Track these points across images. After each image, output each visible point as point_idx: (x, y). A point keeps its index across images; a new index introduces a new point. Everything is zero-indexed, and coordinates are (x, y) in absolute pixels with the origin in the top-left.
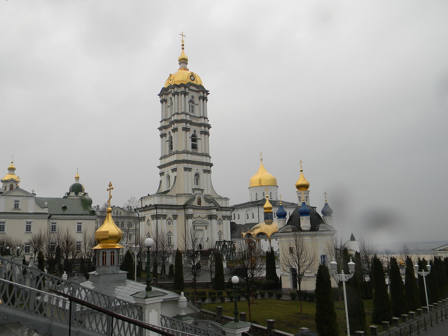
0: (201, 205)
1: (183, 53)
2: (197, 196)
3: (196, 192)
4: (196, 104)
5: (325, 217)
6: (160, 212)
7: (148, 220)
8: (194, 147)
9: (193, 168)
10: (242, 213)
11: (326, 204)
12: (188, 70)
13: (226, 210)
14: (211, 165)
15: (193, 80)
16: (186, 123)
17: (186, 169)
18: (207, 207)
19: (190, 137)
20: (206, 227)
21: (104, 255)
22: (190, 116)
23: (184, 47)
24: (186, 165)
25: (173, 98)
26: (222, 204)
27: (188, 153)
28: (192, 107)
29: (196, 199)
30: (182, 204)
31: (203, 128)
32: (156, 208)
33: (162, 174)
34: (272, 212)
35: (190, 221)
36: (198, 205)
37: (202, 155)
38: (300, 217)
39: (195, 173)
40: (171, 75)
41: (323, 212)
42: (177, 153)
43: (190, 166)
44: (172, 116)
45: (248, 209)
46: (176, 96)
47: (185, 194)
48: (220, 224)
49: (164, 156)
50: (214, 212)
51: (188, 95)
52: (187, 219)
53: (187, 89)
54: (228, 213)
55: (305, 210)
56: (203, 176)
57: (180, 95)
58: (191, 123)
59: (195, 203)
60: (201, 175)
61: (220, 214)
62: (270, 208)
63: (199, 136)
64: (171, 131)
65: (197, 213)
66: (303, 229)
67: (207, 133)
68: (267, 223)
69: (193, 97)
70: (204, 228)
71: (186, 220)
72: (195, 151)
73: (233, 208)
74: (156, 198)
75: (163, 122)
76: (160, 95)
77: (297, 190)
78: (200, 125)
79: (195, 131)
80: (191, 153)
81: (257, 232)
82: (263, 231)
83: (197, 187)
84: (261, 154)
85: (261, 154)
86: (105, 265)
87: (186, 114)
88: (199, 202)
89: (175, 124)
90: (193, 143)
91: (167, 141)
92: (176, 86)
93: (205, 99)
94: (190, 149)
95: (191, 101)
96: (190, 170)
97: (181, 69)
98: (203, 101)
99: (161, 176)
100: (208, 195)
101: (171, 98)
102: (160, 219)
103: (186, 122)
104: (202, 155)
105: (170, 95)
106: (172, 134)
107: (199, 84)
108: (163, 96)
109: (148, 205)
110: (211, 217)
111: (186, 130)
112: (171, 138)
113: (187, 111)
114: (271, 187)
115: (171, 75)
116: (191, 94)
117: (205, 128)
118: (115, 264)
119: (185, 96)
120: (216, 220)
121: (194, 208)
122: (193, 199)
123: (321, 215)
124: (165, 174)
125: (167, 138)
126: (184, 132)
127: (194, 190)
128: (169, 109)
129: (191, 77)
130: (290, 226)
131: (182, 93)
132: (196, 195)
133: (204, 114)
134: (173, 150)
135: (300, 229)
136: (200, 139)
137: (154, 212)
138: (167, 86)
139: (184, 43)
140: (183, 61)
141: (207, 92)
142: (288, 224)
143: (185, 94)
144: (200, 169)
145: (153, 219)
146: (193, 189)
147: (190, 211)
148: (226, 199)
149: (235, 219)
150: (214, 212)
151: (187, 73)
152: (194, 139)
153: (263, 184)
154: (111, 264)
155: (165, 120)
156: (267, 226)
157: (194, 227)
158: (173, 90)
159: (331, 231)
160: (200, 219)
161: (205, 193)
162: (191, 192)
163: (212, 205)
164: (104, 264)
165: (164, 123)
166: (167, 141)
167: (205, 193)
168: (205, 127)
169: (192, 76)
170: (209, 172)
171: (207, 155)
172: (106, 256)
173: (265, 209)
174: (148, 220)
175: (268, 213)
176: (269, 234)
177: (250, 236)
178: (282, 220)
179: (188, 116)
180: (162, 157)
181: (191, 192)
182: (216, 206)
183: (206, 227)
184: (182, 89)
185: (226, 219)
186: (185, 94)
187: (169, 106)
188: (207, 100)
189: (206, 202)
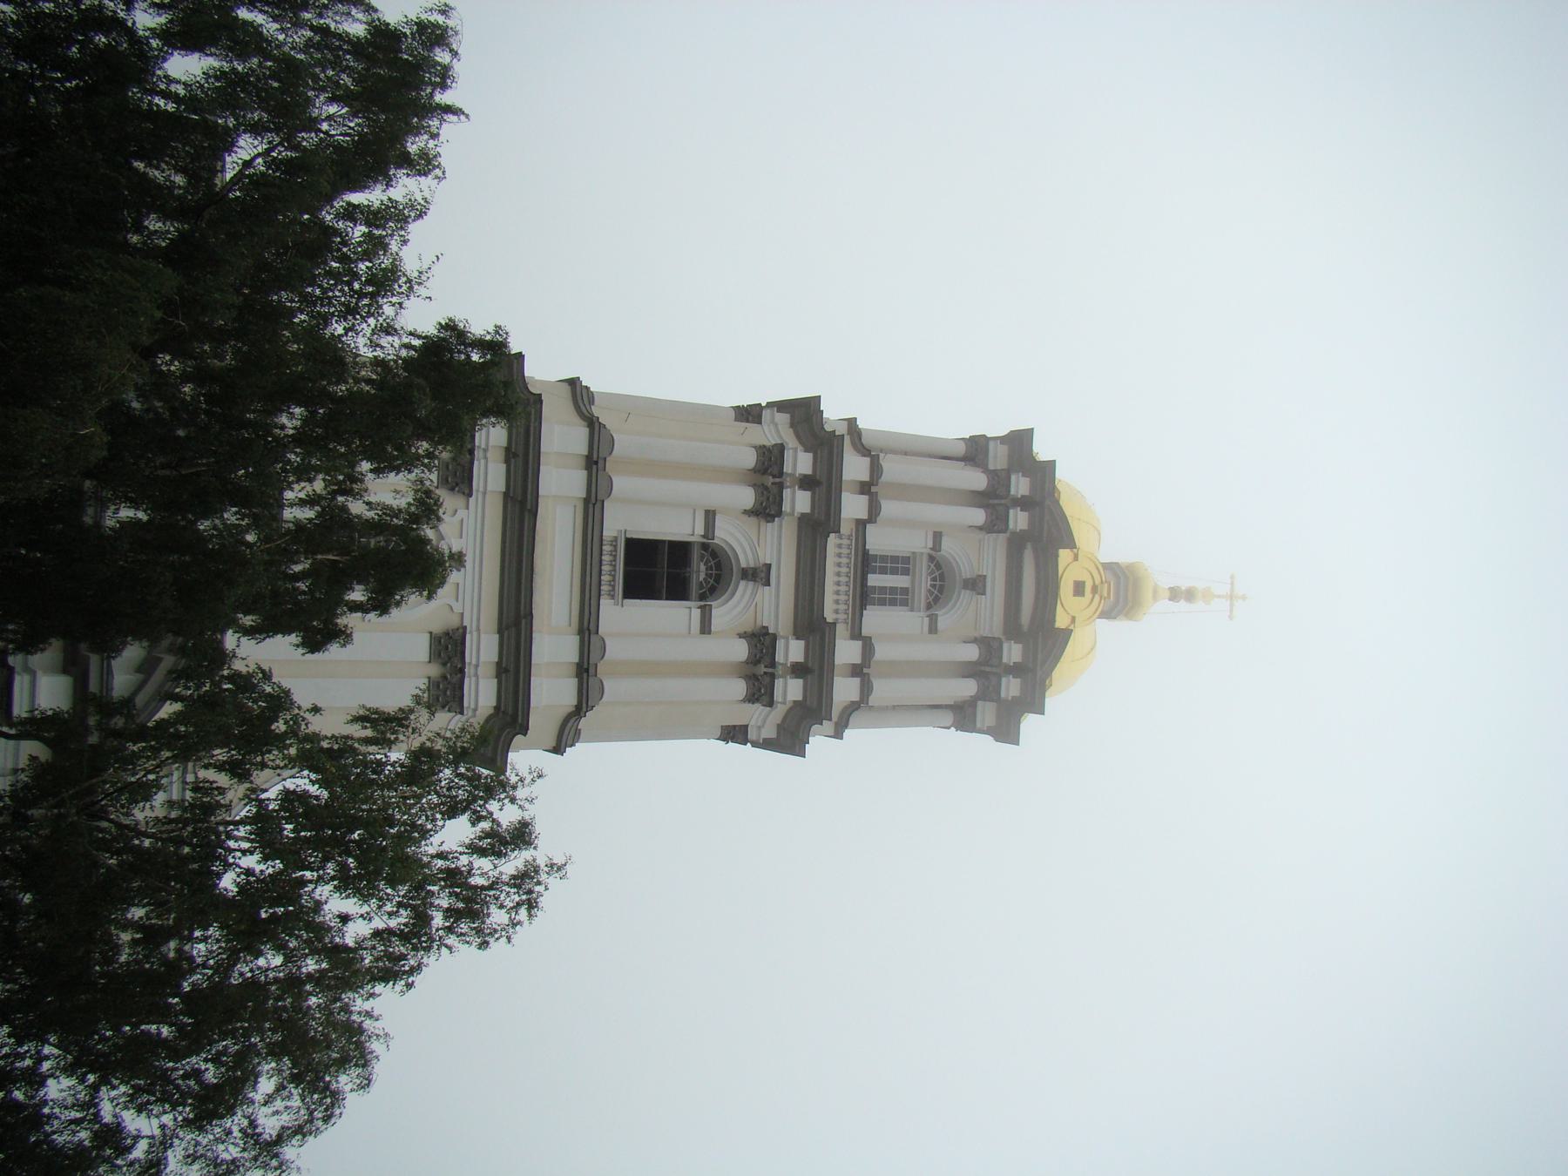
4: (933, 620)
19: (710, 516)
23: (1183, 604)
37: (587, 628)
53: (1019, 520)
58: (817, 527)
69: (976, 585)
78: (812, 626)
79: (759, 575)
80: (593, 505)
95: (943, 583)
103: (824, 484)
104: (587, 628)
126: (749, 459)
136: (705, 628)
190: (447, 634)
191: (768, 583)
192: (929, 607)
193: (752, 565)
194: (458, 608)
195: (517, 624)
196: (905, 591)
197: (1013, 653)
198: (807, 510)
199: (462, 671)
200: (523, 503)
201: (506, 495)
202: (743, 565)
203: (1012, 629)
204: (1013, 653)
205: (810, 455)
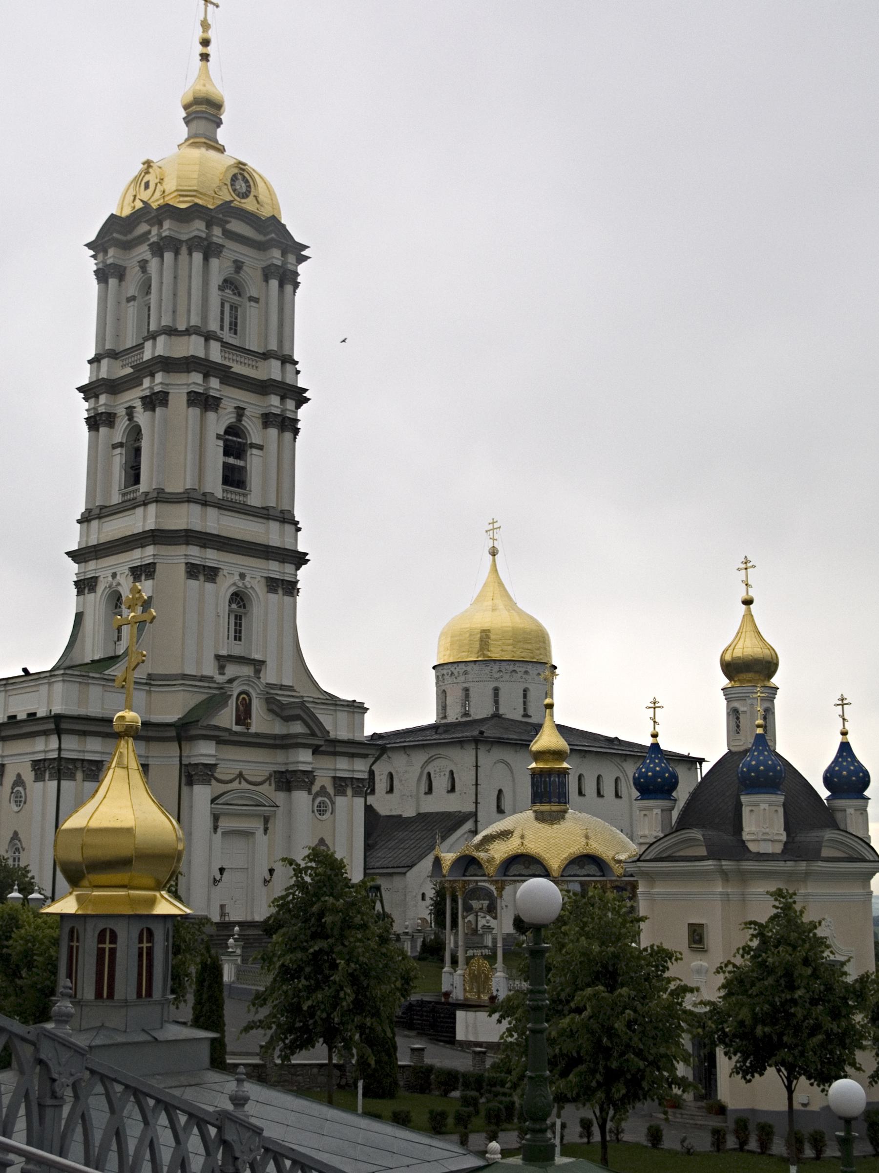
0: (248, 726)
1: (205, 74)
2: (236, 689)
3: (232, 670)
5: (840, 803)
6: (73, 747)
7: (19, 781)
8: (234, 478)
9: (225, 569)
10: (407, 768)
11: (845, 747)
12: (221, 150)
13: (353, 756)
14: (301, 559)
15: (245, 195)
16: (206, 376)
17: (193, 571)
18: (275, 737)
19: (218, 437)
20: (266, 820)
21: (107, 946)
22: (225, 345)
23: (210, 50)
24: (195, 554)
25: (153, 265)
26: (337, 727)
27: (205, 501)
28: (234, 308)
29: (232, 703)
30: (172, 717)
31: (275, 400)
32: (59, 732)
33: (84, 586)
34: (564, 773)
35: (202, 794)
36: (236, 728)
37: (264, 514)
38: (744, 799)
39: (233, 589)
40: (148, 164)
41: (828, 781)
42: (161, 497)
43: (211, 557)
44: (146, 339)
45: (433, 752)
46: (168, 256)
47: (184, 677)
48: (322, 812)
49: (102, 508)
50: (304, 759)
51: (218, 255)
52: (190, 783)
53: (217, 231)
54: (359, 768)
55: (768, 768)
56: (264, 603)
57: (184, 250)
59: (226, 718)
60: (255, 603)
61: (326, 769)
62: (558, 755)
63: (254, 432)
64: (138, 404)
65: (233, 761)
66: (753, 847)
67: (289, 426)
68: (540, 817)
69: (238, 266)
70: (257, 825)
71: (185, 789)
72: (234, 495)
73: (383, 745)
74: (59, 687)
75: (105, 362)
76: (97, 246)
77: (725, 682)
79: (240, 412)
80: (221, 506)
81: (500, 851)
82: (533, 847)
83: (237, 650)
84: (494, 527)
85: (494, 527)
86: (111, 995)
87: (208, 337)
88: (244, 715)
89: (159, 377)
90: (231, 460)
91: (114, 446)
92: (168, 211)
93: (289, 280)
94: (214, 485)
96: (211, 574)
97: (193, 140)
98: (281, 286)
99: (80, 593)
100: (282, 687)
101: (143, 265)
102: (72, 777)
104: (264, 514)
105: (143, 251)
106: (142, 417)
107: (266, 212)
108: (111, 252)
109: (22, 716)
110: (287, 781)
111: (204, 402)
112: (136, 432)
113: (213, 326)
114: (529, 667)
115: (148, 164)
116: (234, 251)
117: (284, 400)
118: (157, 994)
119: (206, 259)
120: (310, 793)
121: (223, 738)
122: (216, 700)
123: (824, 793)
124: (101, 587)
125: (119, 433)
127: (222, 661)
128: (131, 310)
129: (234, 178)
130: (696, 834)
131: (194, 244)
132: (231, 681)
133: (280, 342)
134: (143, 487)
135: (738, 849)
136: (261, 448)
137: (46, 747)
138: (127, 212)
139: (211, 34)
140: (204, 113)
141: (298, 252)
142: (684, 823)
143: (210, 251)
144: (256, 571)
145: (39, 777)
146: (218, 657)
147: (204, 751)
148: (357, 709)
149: (373, 792)
150: (304, 759)
151: (218, 165)
152: (235, 444)
153: (495, 653)
154: (139, 995)
155: (113, 355)
156: (545, 830)
157: (216, 818)
158: (155, 231)
159: (864, 860)
160: (245, 785)
161: (270, 676)
162: (209, 669)
163: (297, 728)
164: (105, 989)
165: (105, 370)
166: (114, 446)
167: (270, 676)
168: (283, 398)
169: (241, 178)
170: (291, 588)
171: (288, 520)
172: (113, 952)
173: (539, 756)
174: (19, 781)
175: (550, 772)
176: (555, 864)
177: (472, 869)
178: (656, 806)
179: (215, 346)
180: (88, 511)
181: (209, 669)
182: (313, 734)
183: (266, 820)
184: (198, 227)
185: (349, 792)
186: (210, 251)
187: (133, 298)
188: (296, 285)
189: (270, 717)
190: (268, 586)
191: (244, 409)
192: (240, 295)
193: (234, 415)
194: (259, 578)
195: (268, 552)
196: (231, 307)
197: (275, 256)
198: (218, 380)
199: (283, 580)
200: (224, 543)
201: (218, 550)
202: (234, 420)
203: (261, 247)
204: (275, 256)
205: (193, 374)
